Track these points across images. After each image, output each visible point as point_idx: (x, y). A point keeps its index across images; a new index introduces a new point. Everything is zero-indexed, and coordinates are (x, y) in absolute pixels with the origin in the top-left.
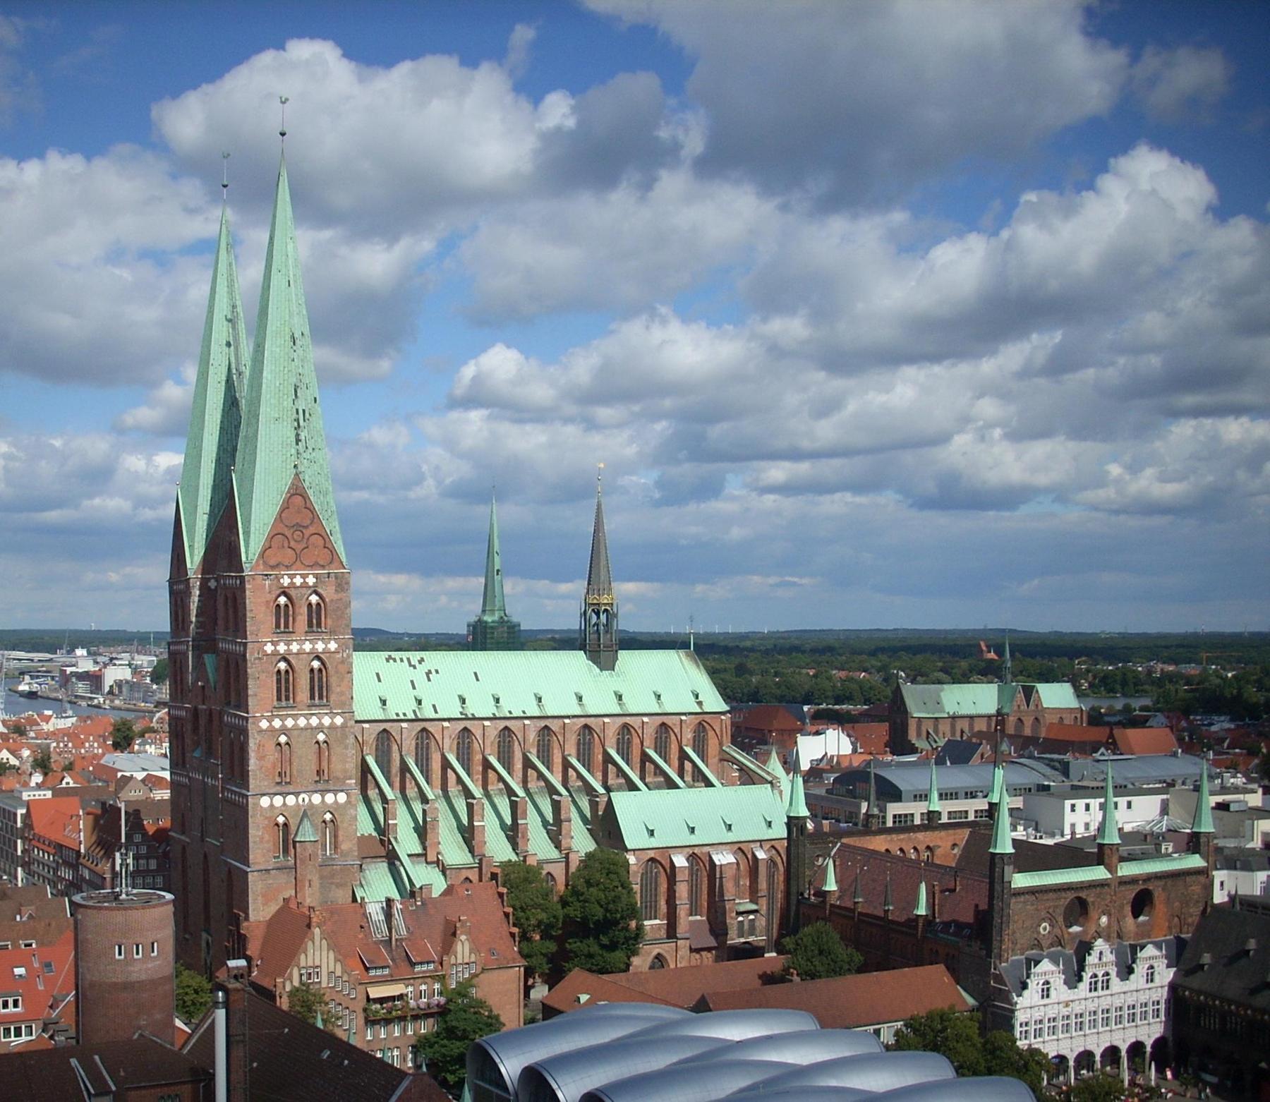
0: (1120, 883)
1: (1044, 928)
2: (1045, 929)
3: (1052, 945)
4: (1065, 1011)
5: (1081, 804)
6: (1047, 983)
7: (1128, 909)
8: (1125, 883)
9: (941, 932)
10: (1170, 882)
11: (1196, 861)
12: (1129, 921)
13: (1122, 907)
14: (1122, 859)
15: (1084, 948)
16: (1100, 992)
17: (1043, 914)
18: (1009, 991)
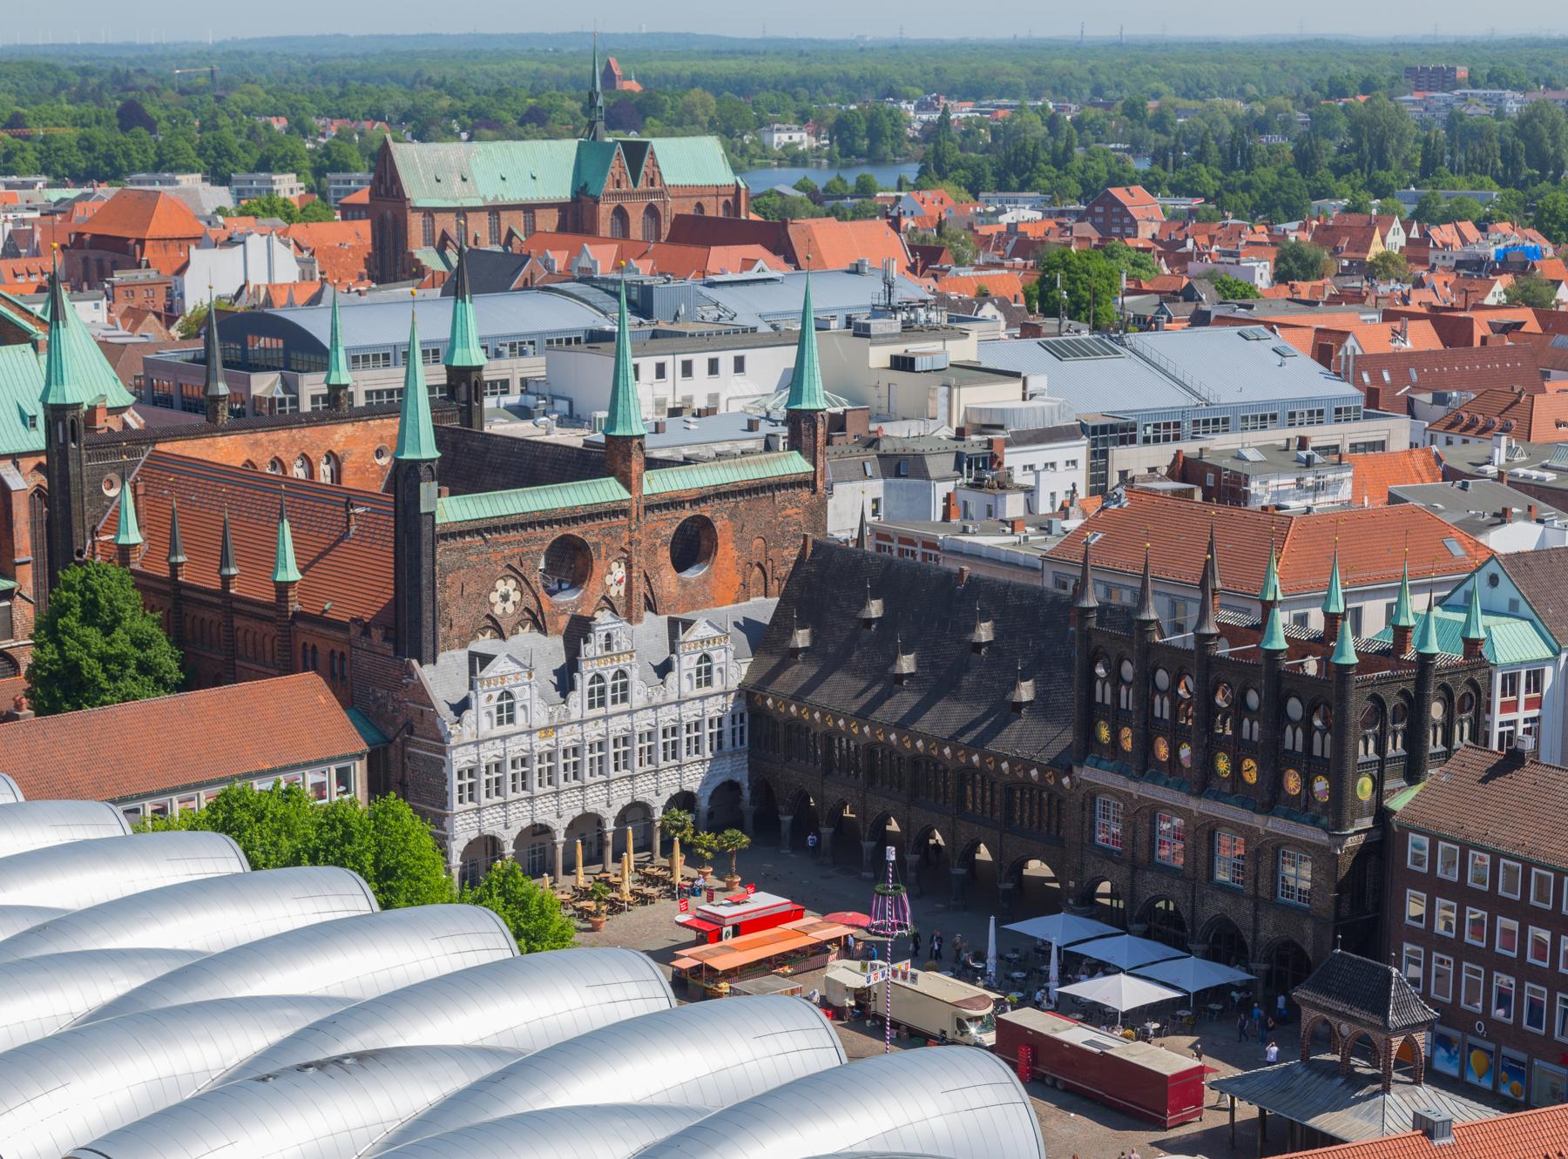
0: (649, 508)
4: (541, 744)
5: (673, 363)
6: (509, 695)
7: (664, 555)
8: (659, 507)
10: (742, 503)
11: (797, 464)
13: (652, 550)
14: (652, 464)
15: (579, 630)
16: (612, 709)
17: (500, 569)
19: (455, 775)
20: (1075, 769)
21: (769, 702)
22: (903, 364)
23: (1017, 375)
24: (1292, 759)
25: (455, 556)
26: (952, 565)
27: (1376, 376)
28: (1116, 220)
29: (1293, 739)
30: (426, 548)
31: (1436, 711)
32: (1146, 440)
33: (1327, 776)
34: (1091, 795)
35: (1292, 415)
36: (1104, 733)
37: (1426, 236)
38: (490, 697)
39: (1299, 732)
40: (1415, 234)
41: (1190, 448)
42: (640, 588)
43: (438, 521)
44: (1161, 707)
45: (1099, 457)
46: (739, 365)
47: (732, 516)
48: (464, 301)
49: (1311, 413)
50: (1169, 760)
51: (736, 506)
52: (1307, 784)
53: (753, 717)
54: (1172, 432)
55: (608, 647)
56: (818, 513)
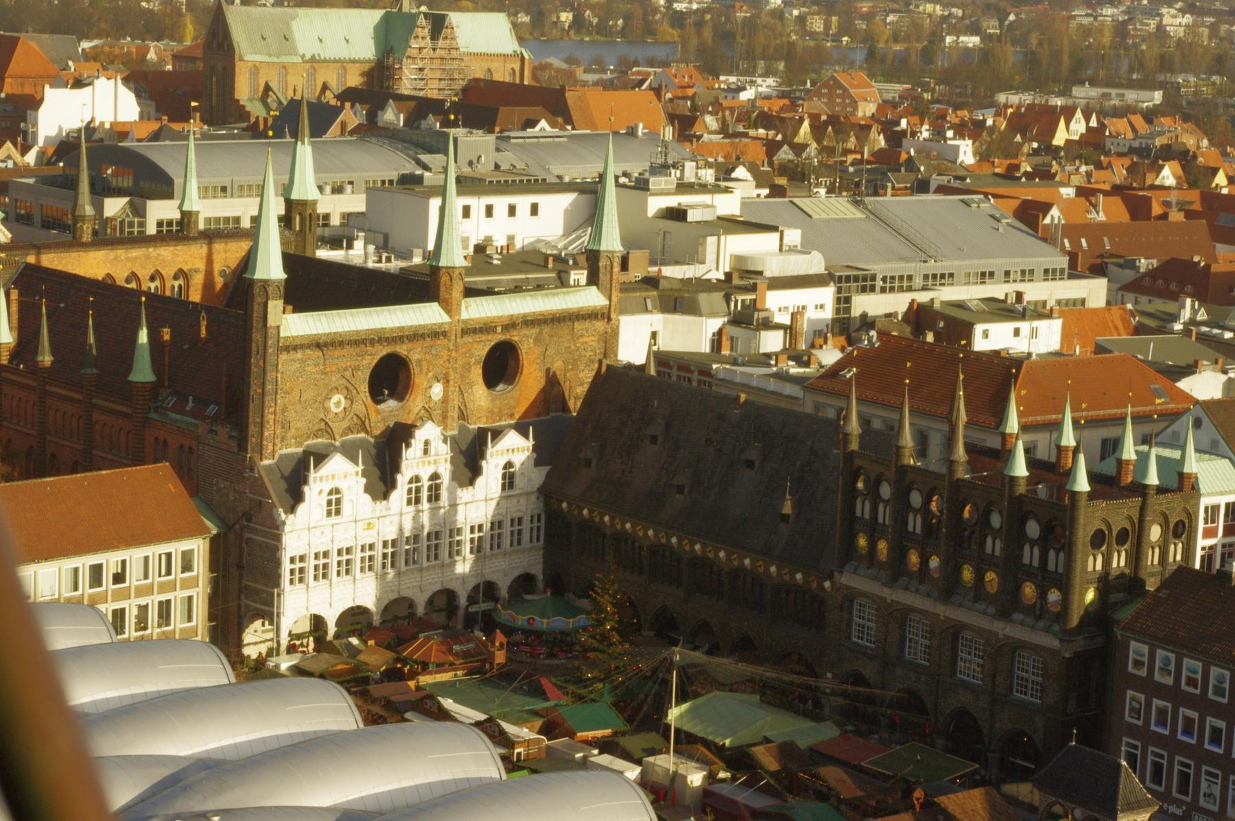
1: (337, 403)
2: (338, 403)
3: (349, 430)
6: (337, 491)
7: (477, 373)
8: (474, 331)
9: (173, 410)
10: (546, 329)
11: (593, 298)
12: (480, 395)
13: (467, 368)
14: (471, 292)
15: (399, 435)
18: (273, 506)
19: (288, 560)
20: (836, 574)
21: (564, 505)
22: (677, 214)
23: (773, 229)
24: (1029, 573)
25: (297, 365)
26: (723, 391)
27: (1076, 243)
28: (838, 100)
29: (1031, 556)
30: (271, 358)
31: (1155, 533)
32: (883, 290)
33: (1060, 590)
34: (850, 597)
35: (1007, 273)
36: (862, 542)
37: (1102, 126)
38: (321, 492)
39: (1036, 551)
40: (1094, 123)
41: (923, 297)
42: (456, 401)
43: (282, 334)
44: (915, 524)
45: (843, 302)
46: (534, 210)
47: (537, 340)
48: (303, 143)
49: (1023, 272)
50: (920, 570)
51: (541, 332)
52: (1043, 595)
53: (548, 517)
54: (905, 284)
55: (426, 452)
56: (610, 340)
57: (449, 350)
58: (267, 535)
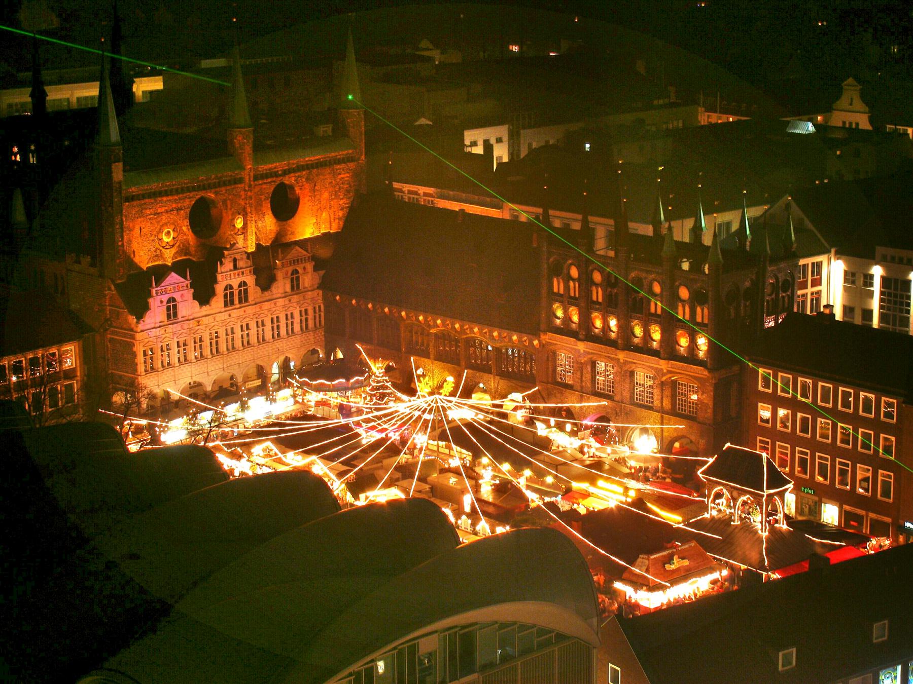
6: (174, 300)
24: (681, 324)
57: (245, 191)
58: (125, 335)
